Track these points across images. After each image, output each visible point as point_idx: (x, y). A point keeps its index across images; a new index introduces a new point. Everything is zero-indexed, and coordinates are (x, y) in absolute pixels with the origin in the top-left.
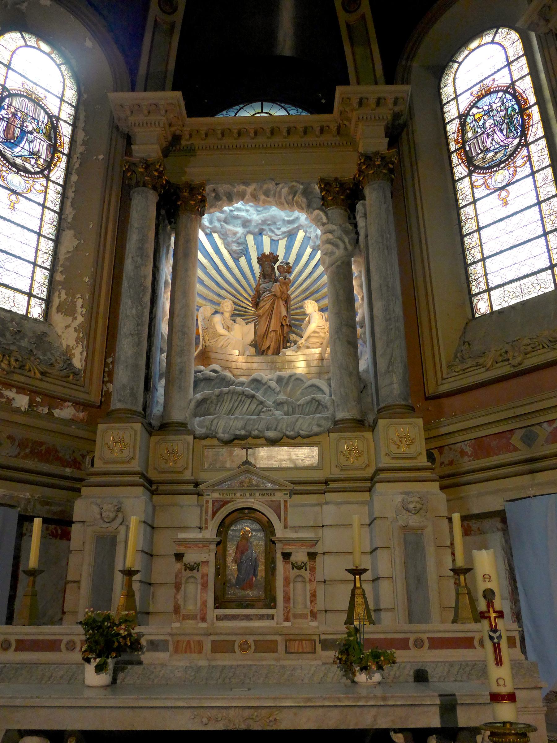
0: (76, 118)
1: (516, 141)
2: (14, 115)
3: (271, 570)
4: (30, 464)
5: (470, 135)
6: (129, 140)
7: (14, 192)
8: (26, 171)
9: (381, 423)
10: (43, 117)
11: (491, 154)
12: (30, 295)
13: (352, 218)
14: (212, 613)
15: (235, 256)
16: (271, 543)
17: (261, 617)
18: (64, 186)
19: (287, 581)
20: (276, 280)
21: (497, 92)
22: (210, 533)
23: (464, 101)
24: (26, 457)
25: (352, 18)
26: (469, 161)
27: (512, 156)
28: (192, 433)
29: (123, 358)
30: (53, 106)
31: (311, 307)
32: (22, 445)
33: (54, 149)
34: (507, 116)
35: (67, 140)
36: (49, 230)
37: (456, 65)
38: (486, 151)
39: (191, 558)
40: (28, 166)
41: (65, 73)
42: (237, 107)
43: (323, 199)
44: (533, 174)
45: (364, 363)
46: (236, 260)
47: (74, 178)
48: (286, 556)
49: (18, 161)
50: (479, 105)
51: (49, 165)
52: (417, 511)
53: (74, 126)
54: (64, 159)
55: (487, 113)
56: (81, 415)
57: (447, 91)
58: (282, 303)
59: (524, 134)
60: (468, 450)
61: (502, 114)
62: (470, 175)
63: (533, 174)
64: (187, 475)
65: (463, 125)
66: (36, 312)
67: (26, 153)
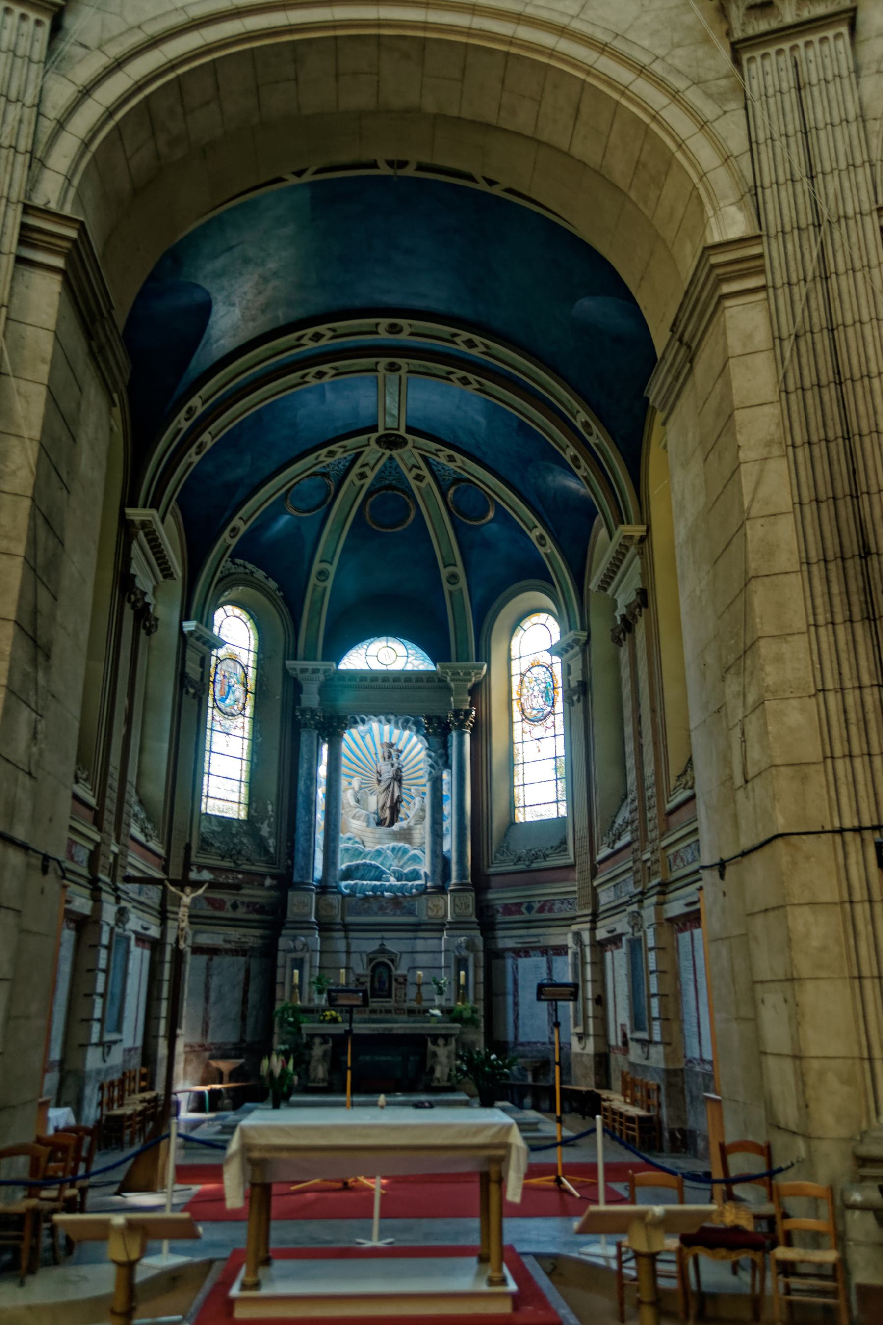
1: (549, 709)
2: (224, 676)
5: (525, 691)
8: (233, 715)
10: (239, 670)
15: (362, 734)
16: (390, 976)
17: (386, 1002)
19: (396, 989)
20: (394, 872)
21: (543, 666)
22: (369, 972)
23: (525, 664)
24: (250, 912)
25: (453, 588)
26: (523, 711)
27: (545, 717)
28: (340, 892)
29: (301, 848)
30: (244, 662)
32: (249, 905)
33: (247, 692)
34: (546, 687)
40: (233, 711)
41: (252, 637)
42: (369, 641)
46: (363, 738)
48: (396, 980)
49: (228, 710)
56: (275, 882)
58: (396, 784)
60: (501, 910)
61: (544, 685)
65: (522, 682)
67: (232, 702)
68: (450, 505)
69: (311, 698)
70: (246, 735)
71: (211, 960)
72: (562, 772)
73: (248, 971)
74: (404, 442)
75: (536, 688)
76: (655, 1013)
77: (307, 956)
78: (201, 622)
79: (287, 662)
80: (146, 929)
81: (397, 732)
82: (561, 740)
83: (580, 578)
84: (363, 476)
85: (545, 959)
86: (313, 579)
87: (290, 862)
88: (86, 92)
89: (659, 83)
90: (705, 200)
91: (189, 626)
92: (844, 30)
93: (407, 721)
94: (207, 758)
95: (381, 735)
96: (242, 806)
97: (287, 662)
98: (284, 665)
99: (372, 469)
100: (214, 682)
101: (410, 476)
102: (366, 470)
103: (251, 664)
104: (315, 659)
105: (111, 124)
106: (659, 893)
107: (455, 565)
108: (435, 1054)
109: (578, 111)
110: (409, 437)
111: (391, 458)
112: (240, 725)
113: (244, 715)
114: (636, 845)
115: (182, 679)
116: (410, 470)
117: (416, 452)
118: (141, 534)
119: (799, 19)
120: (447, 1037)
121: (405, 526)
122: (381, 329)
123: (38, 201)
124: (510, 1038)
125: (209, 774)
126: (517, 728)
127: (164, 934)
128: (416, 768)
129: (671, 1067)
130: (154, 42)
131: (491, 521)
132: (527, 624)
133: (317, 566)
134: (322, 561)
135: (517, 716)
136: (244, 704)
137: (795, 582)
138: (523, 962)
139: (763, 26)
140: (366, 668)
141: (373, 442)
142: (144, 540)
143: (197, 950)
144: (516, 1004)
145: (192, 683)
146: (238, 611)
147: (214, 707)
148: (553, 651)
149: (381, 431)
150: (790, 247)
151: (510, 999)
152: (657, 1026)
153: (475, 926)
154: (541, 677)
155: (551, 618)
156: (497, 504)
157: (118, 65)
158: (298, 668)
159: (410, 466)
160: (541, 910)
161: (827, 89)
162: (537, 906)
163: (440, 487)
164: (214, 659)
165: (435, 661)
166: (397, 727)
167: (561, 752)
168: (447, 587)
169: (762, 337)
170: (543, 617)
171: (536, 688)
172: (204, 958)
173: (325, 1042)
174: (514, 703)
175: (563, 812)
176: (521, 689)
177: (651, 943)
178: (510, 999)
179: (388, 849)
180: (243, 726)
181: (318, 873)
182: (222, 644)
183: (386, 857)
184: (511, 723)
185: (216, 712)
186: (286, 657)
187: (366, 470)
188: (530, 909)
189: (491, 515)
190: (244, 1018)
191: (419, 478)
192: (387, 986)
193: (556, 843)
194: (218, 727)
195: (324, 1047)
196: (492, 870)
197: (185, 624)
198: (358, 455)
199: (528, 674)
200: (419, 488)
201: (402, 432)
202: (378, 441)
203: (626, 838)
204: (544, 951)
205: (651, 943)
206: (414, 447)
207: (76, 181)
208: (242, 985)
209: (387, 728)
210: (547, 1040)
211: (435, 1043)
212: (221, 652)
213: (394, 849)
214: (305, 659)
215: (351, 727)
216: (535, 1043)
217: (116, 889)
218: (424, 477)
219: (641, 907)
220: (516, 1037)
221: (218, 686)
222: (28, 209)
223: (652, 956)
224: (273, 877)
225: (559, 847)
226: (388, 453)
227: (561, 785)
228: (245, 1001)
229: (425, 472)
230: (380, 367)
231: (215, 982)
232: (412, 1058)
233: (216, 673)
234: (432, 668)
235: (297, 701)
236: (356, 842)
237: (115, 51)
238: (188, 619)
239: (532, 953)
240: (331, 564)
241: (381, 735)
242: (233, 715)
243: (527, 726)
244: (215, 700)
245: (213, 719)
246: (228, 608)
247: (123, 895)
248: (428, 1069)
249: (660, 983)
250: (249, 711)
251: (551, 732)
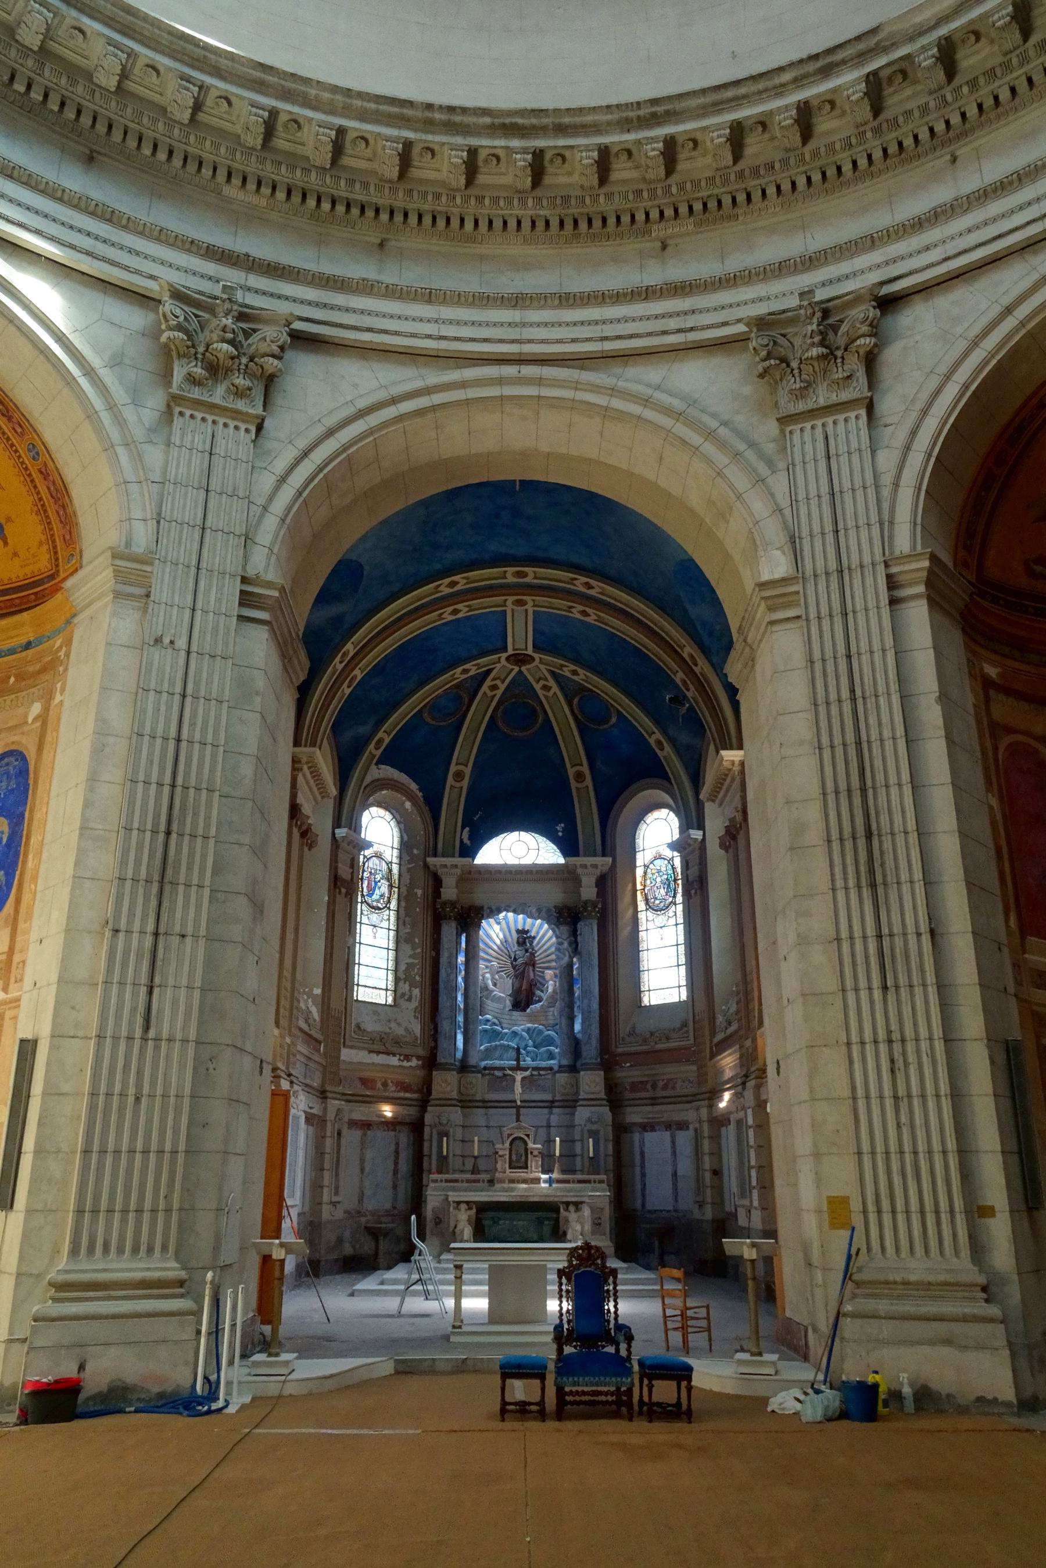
0: (400, 857)
1: (671, 899)
3: (527, 1157)
4: (402, 1094)
5: (648, 882)
6: (437, 882)
7: (375, 926)
8: (379, 909)
9: (582, 1073)
10: (385, 867)
11: (657, 902)
12: (387, 990)
13: (574, 933)
14: (508, 1170)
16: (526, 1150)
18: (398, 911)
25: (580, 785)
26: (647, 900)
31: (549, 973)
33: (391, 886)
34: (667, 879)
35: (396, 877)
36: (392, 946)
37: (645, 826)
38: (656, 899)
39: (501, 1153)
42: (502, 836)
43: (558, 918)
44: (677, 925)
45: (577, 1027)
47: (403, 904)
49: (375, 904)
50: (656, 862)
51: (389, 902)
52: (596, 1122)
53: (400, 864)
54: (396, 890)
55: (659, 871)
57: (639, 842)
58: (531, 969)
59: (674, 897)
62: (647, 910)
63: (677, 925)
64: (479, 1097)
65: (645, 873)
66: (390, 1001)
68: (576, 712)
69: (449, 892)
70: (392, 927)
71: (365, 1134)
72: (682, 960)
73: (397, 1144)
74: (533, 659)
75: (659, 879)
76: (754, 1183)
77: (451, 1130)
78: (350, 829)
79: (428, 859)
80: (311, 1108)
81: (529, 921)
82: (681, 927)
83: (697, 781)
84: (494, 688)
85: (668, 1133)
86: (450, 781)
87: (433, 1044)
88: (283, 480)
89: (722, 445)
90: (758, 542)
91: (341, 832)
92: (863, 413)
93: (539, 911)
94: (357, 950)
95: (516, 921)
96: (389, 993)
97: (428, 859)
98: (425, 862)
99: (503, 682)
100: (362, 879)
101: (537, 687)
102: (498, 682)
103: (395, 860)
104: (453, 856)
105: (301, 499)
106: (757, 1078)
107: (582, 765)
108: (567, 1220)
109: (661, 459)
110: (537, 656)
111: (520, 672)
112: (386, 917)
113: (389, 908)
114: (742, 1033)
115: (336, 881)
116: (538, 681)
117: (542, 667)
118: (305, 768)
119: (830, 402)
120: (578, 1205)
121: (535, 729)
122: (508, 575)
123: (251, 573)
124: (638, 1205)
125: (359, 964)
126: (642, 916)
127: (325, 1109)
128: (548, 952)
129: (768, 1228)
130: (331, 433)
131: (614, 725)
132: (650, 818)
133: (453, 768)
134: (457, 764)
135: (641, 905)
136: (389, 898)
137: (821, 853)
138: (649, 1136)
139: (801, 406)
140: (501, 862)
141: (503, 660)
142: (309, 776)
143: (353, 1124)
144: (643, 1175)
145: (343, 880)
146: (382, 812)
147: (362, 903)
148: (673, 846)
149: (510, 651)
150: (820, 587)
151: (638, 1169)
152: (755, 1194)
153: (605, 1102)
154: (663, 869)
155: (671, 814)
156: (619, 712)
157: (305, 454)
158: (438, 864)
159: (537, 677)
160: (665, 1087)
161: (859, 443)
162: (661, 1084)
163: (565, 696)
164: (361, 857)
165: (565, 854)
166: (531, 916)
167: (681, 939)
168: (573, 784)
169: (798, 659)
170: (664, 812)
171: (659, 879)
172: (359, 1133)
173: (470, 1209)
174: (639, 893)
175: (684, 997)
176: (645, 880)
177: (750, 1122)
178: (638, 1169)
179: (523, 1030)
180: (387, 920)
181: (459, 1055)
182: (369, 845)
183: (522, 1037)
184: (636, 912)
185: (364, 907)
186: (427, 854)
187: (498, 682)
188: (654, 1086)
189: (614, 720)
190: (395, 1187)
191: (546, 688)
192: (523, 1158)
193: (678, 1025)
194: (365, 920)
195: (469, 1212)
196: (620, 1050)
197: (337, 831)
198: (489, 671)
199: (651, 866)
200: (546, 697)
201: (530, 651)
202: (508, 659)
203: (735, 1026)
204: (668, 1126)
205: (750, 1122)
206: (541, 662)
207: (275, 551)
208: (393, 1158)
209: (521, 916)
210: (671, 1208)
211: (567, 1210)
212: (368, 852)
213: (528, 1030)
214: (443, 856)
215: (489, 917)
216: (661, 1211)
217: (289, 1075)
218: (551, 688)
219: (744, 1089)
220: (643, 1205)
221: (366, 883)
222: (244, 580)
223: (751, 1132)
224: (419, 1058)
225: (680, 1029)
226: (517, 669)
227: (683, 970)
228: (396, 1172)
229: (552, 683)
230: (509, 603)
231: (369, 1155)
232: (546, 1222)
233: (364, 871)
234: (561, 860)
235: (437, 893)
236: (494, 1024)
237: (302, 444)
238: (339, 827)
239: (657, 1128)
240: (467, 766)
241: (516, 921)
242: (379, 909)
243: (650, 914)
244: (363, 895)
245: (362, 913)
246: (374, 810)
247: (295, 1081)
248: (561, 1232)
249: (757, 1155)
250: (393, 905)
251: (672, 921)
